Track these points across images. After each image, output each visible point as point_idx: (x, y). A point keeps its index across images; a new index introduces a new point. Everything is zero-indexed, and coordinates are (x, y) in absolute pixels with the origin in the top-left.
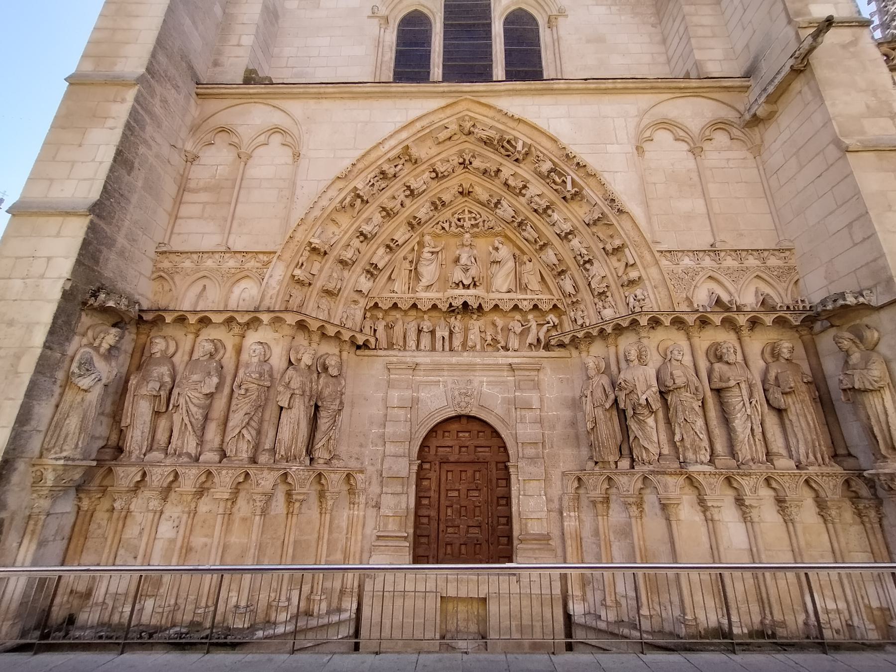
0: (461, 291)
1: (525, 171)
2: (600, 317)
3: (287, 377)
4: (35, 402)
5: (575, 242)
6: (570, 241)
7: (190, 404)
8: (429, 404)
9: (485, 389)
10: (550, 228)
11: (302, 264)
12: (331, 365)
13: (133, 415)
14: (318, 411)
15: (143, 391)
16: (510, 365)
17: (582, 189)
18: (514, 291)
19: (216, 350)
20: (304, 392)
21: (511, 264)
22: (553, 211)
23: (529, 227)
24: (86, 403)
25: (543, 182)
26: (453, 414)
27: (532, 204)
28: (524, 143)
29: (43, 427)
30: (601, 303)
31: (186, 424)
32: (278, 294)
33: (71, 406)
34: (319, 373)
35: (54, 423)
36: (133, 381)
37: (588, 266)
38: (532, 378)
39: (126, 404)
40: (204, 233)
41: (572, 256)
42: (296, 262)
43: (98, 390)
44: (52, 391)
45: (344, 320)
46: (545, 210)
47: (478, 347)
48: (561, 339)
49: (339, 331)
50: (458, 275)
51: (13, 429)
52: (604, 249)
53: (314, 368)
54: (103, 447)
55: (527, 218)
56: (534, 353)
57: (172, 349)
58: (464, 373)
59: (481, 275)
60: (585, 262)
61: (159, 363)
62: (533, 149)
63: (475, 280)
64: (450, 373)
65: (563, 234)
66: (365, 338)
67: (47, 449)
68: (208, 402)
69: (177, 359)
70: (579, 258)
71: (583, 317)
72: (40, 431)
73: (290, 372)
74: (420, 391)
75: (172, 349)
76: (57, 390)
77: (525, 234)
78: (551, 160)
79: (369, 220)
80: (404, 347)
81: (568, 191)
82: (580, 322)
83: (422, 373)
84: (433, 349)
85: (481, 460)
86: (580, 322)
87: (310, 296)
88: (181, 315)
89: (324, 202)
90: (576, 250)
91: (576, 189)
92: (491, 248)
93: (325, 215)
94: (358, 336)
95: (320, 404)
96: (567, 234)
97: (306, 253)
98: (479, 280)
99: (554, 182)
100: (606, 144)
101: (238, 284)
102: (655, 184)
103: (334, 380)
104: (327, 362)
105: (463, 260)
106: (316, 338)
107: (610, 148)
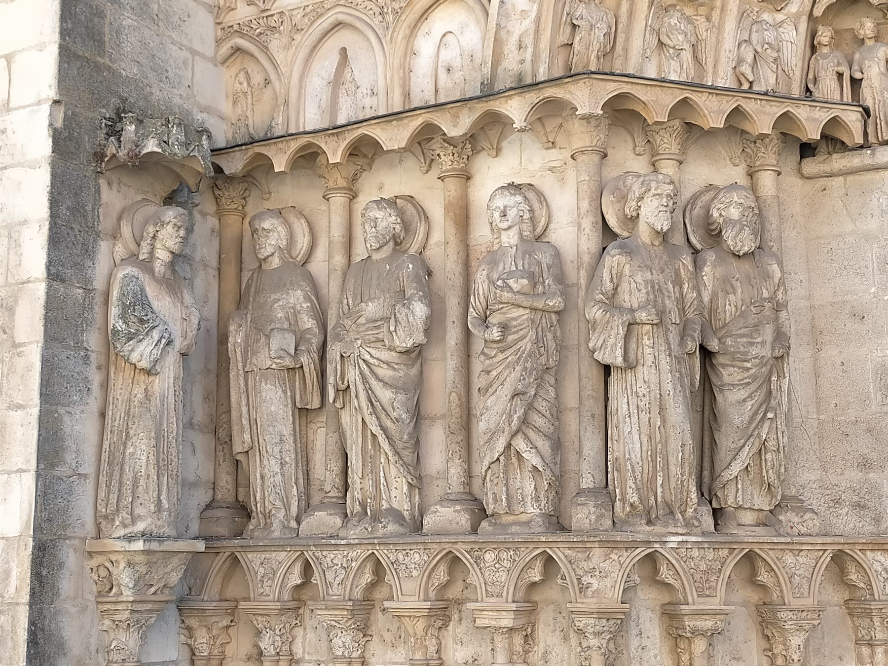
3: (606, 276)
4: (61, 410)
7: (373, 382)
12: (729, 221)
13: (252, 422)
14: (713, 366)
15: (263, 360)
19: (407, 226)
20: (661, 313)
24: (156, 401)
29: (88, 468)
31: (373, 435)
32: (537, 32)
33: (128, 413)
34: (696, 252)
35: (105, 456)
36: (236, 339)
39: (233, 399)
43: (170, 367)
44: (86, 380)
49: (736, 109)
51: (38, 476)
53: (678, 239)
54: (208, 506)
57: (302, 242)
61: (281, 286)
67: (106, 517)
68: (414, 371)
69: (318, 266)
72: (85, 476)
73: (614, 259)
75: (302, 242)
76: (96, 378)
87: (631, 13)
88: (304, 148)
94: (802, 112)
95: (713, 345)
101: (424, 28)
103: (746, 266)
104: (716, 214)
106: (668, 144)
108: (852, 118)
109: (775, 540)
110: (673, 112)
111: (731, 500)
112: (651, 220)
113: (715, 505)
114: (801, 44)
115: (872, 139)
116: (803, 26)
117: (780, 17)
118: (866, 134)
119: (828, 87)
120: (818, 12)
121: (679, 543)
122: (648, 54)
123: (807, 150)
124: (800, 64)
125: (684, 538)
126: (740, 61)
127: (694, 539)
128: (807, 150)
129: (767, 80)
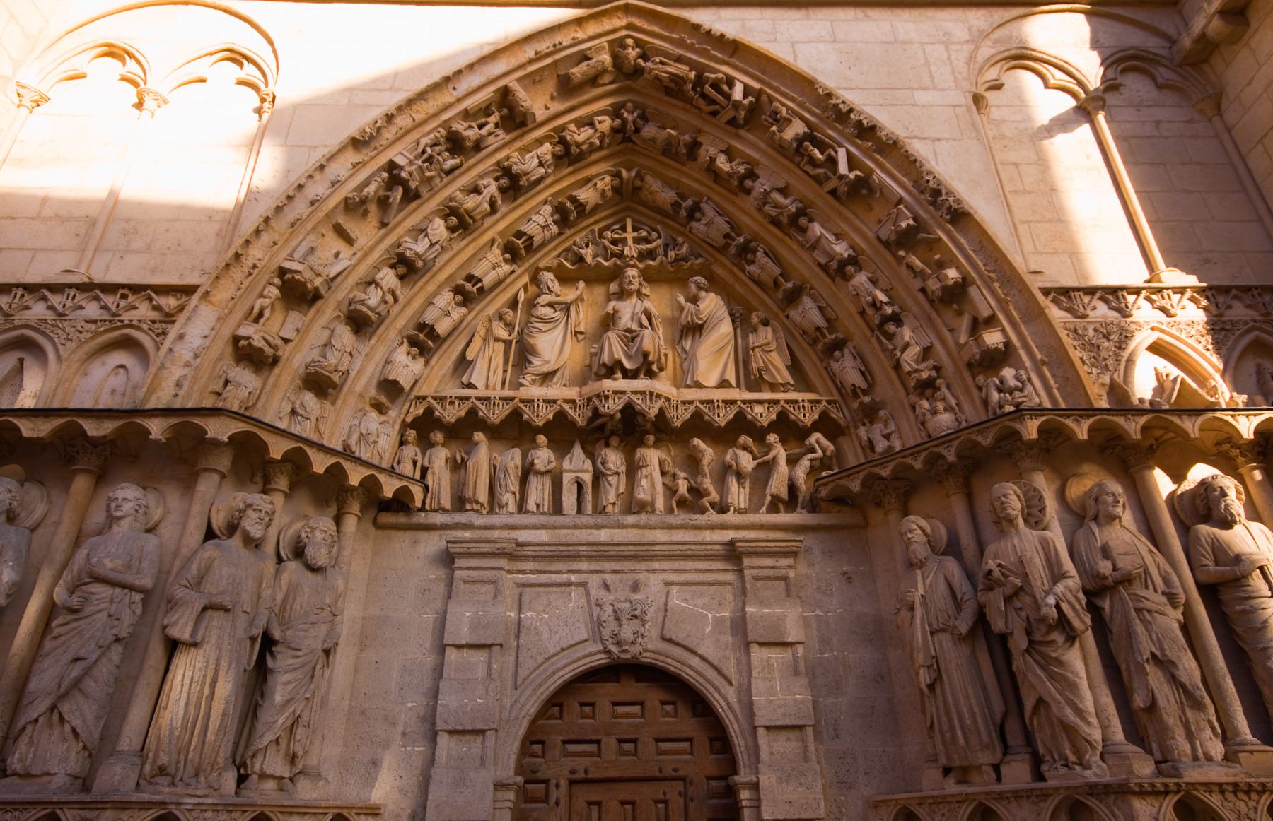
0: (620, 383)
1: (750, 146)
2: (924, 434)
5: (861, 279)
6: (847, 278)
8: (546, 636)
9: (677, 599)
10: (805, 255)
11: (261, 315)
16: (731, 543)
17: (869, 173)
18: (733, 382)
21: (726, 328)
22: (811, 221)
23: (760, 254)
25: (788, 163)
26: (601, 660)
27: (767, 208)
28: (747, 91)
30: (925, 404)
37: (891, 327)
38: (783, 572)
40: (36, 250)
41: (853, 310)
42: (246, 308)
45: (353, 442)
46: (794, 218)
47: (660, 504)
48: (842, 482)
50: (614, 348)
52: (923, 290)
55: (756, 237)
56: (784, 518)
58: (626, 565)
59: (663, 351)
60: (886, 319)
62: (764, 98)
63: (650, 358)
64: (594, 566)
65: (834, 265)
66: (397, 484)
70: (870, 311)
71: (887, 437)
74: (525, 607)
77: (751, 268)
78: (802, 118)
79: (421, 231)
80: (494, 502)
81: (842, 177)
82: (881, 445)
83: (529, 566)
84: (557, 508)
85: (669, 771)
86: (881, 445)
89: (318, 189)
90: (863, 293)
91: (858, 173)
92: (682, 299)
93: (321, 215)
96: (843, 264)
97: (274, 292)
98: (659, 358)
99: (813, 162)
100: (911, 89)
102: (1016, 165)
105: (625, 320)
107: (923, 97)
108: (417, 491)
109: (286, 803)
110: (288, 457)
111: (257, 767)
112: (248, 528)
113: (242, 771)
114: (394, 438)
115: (427, 507)
116: (397, 427)
117: (383, 418)
118: (424, 503)
119: (407, 468)
120: (409, 419)
121: (195, 804)
122: (282, 415)
123: (386, 506)
124: (390, 449)
125: (200, 800)
126: (349, 436)
127: (209, 801)
128: (386, 506)
129: (365, 454)
